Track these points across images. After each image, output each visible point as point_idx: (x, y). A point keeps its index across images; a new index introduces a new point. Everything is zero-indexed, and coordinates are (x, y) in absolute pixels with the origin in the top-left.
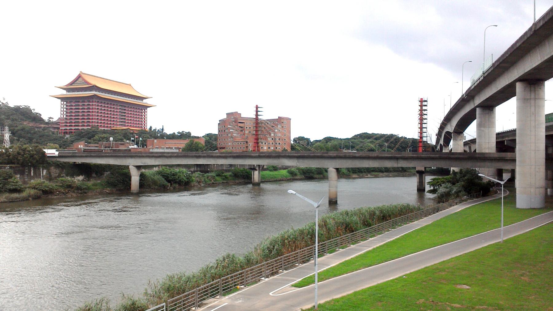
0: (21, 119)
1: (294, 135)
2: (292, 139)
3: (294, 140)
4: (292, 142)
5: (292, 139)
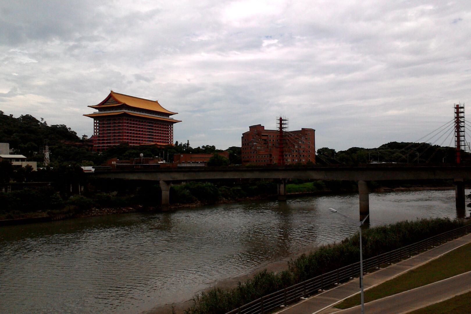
0: (24, 131)
1: (319, 145)
2: (316, 150)
3: (319, 151)
4: (317, 154)
5: (316, 150)
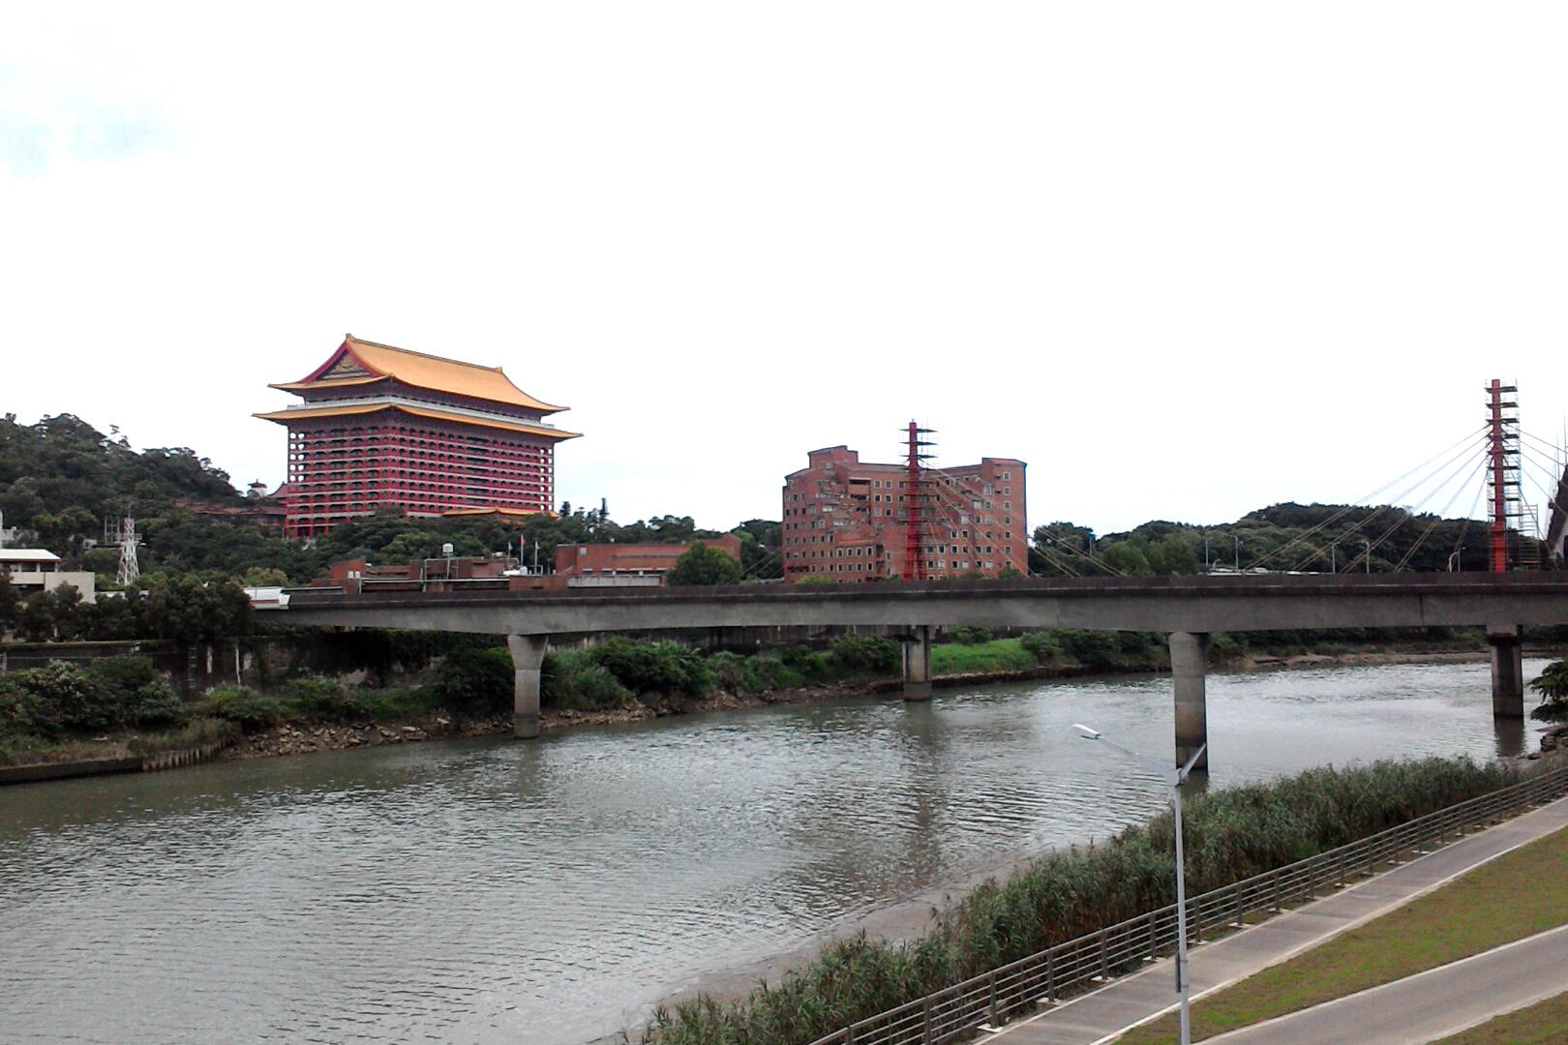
0: (50, 473)
1: (1039, 514)
2: (1031, 532)
3: (1040, 535)
4: (1032, 544)
5: (1031, 532)
